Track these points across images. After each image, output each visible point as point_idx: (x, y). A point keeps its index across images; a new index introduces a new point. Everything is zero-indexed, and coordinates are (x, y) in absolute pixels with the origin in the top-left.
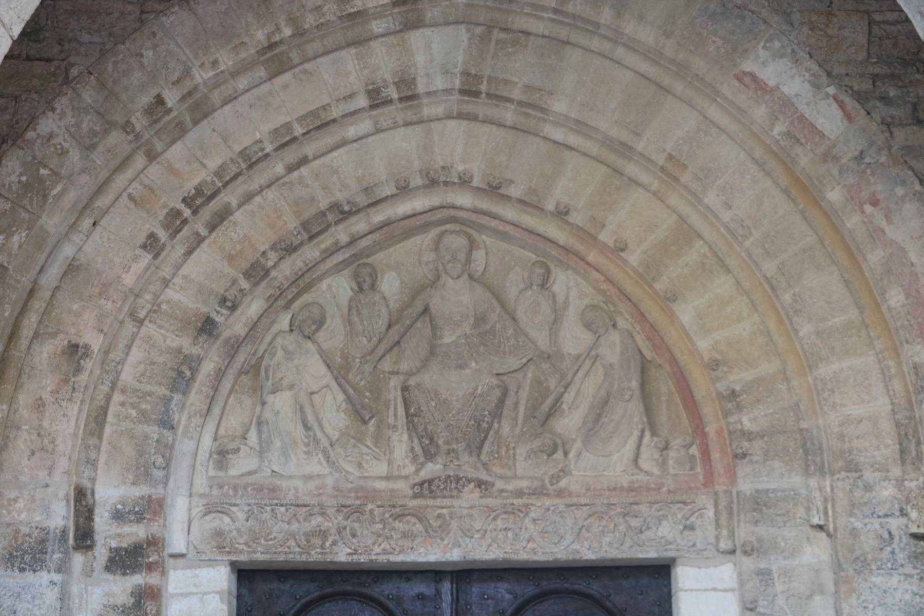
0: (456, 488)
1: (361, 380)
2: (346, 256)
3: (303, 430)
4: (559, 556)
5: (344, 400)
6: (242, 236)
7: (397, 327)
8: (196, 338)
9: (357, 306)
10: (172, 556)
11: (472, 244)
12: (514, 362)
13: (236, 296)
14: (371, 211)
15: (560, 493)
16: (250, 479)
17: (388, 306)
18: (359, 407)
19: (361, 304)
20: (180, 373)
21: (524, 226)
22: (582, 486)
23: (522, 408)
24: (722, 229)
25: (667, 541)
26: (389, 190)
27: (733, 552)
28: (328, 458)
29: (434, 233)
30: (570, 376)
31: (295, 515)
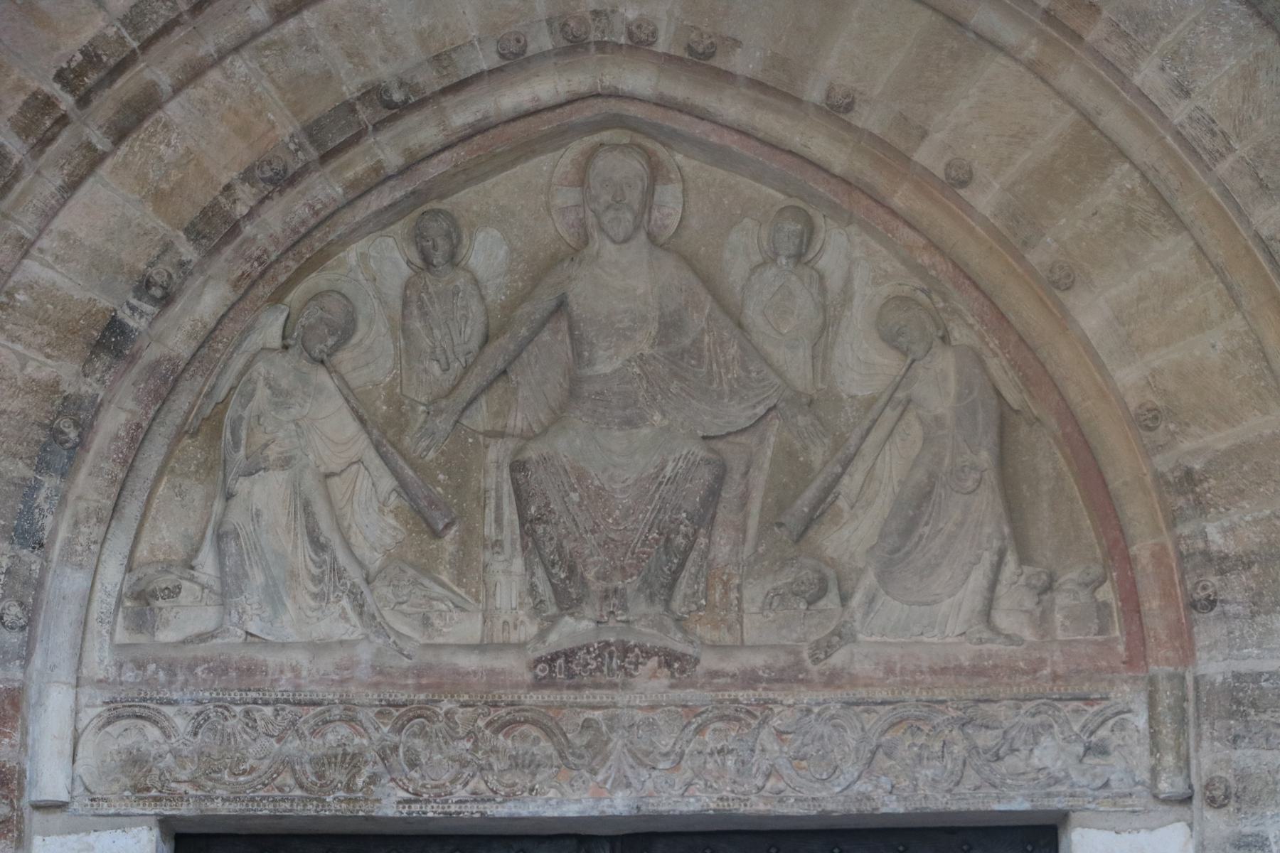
0: (620, 668)
1: (428, 449)
2: (398, 194)
3: (309, 550)
4: (830, 807)
5: (394, 490)
6: (181, 152)
7: (503, 341)
8: (88, 361)
9: (420, 299)
10: (39, 807)
11: (656, 172)
12: (739, 414)
13: (170, 276)
14: (449, 101)
15: (832, 679)
16: (201, 650)
17: (482, 298)
18: (423, 503)
19: (428, 293)
20: (56, 434)
21: (760, 135)
22: (877, 664)
23: (755, 508)
24: (1169, 139)
25: (1049, 776)
26: (485, 59)
27: (1187, 800)
28: (360, 608)
29: (576, 148)
30: (854, 440)
31: (293, 723)
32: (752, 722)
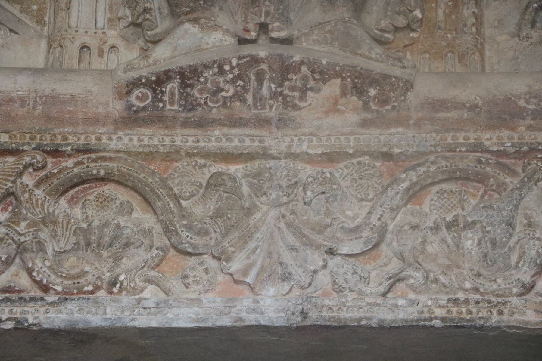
0: (274, 96)
32: (508, 180)
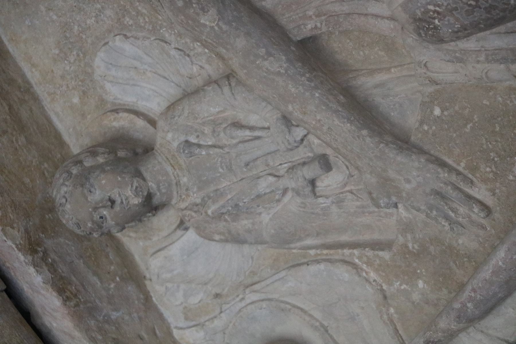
9: (219, 216)
19: (203, 204)
